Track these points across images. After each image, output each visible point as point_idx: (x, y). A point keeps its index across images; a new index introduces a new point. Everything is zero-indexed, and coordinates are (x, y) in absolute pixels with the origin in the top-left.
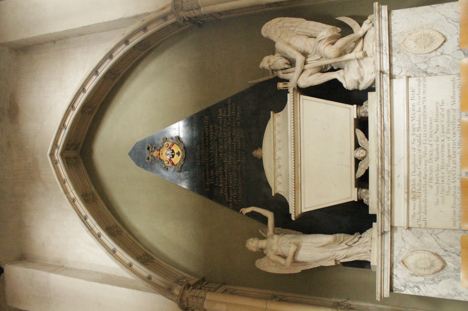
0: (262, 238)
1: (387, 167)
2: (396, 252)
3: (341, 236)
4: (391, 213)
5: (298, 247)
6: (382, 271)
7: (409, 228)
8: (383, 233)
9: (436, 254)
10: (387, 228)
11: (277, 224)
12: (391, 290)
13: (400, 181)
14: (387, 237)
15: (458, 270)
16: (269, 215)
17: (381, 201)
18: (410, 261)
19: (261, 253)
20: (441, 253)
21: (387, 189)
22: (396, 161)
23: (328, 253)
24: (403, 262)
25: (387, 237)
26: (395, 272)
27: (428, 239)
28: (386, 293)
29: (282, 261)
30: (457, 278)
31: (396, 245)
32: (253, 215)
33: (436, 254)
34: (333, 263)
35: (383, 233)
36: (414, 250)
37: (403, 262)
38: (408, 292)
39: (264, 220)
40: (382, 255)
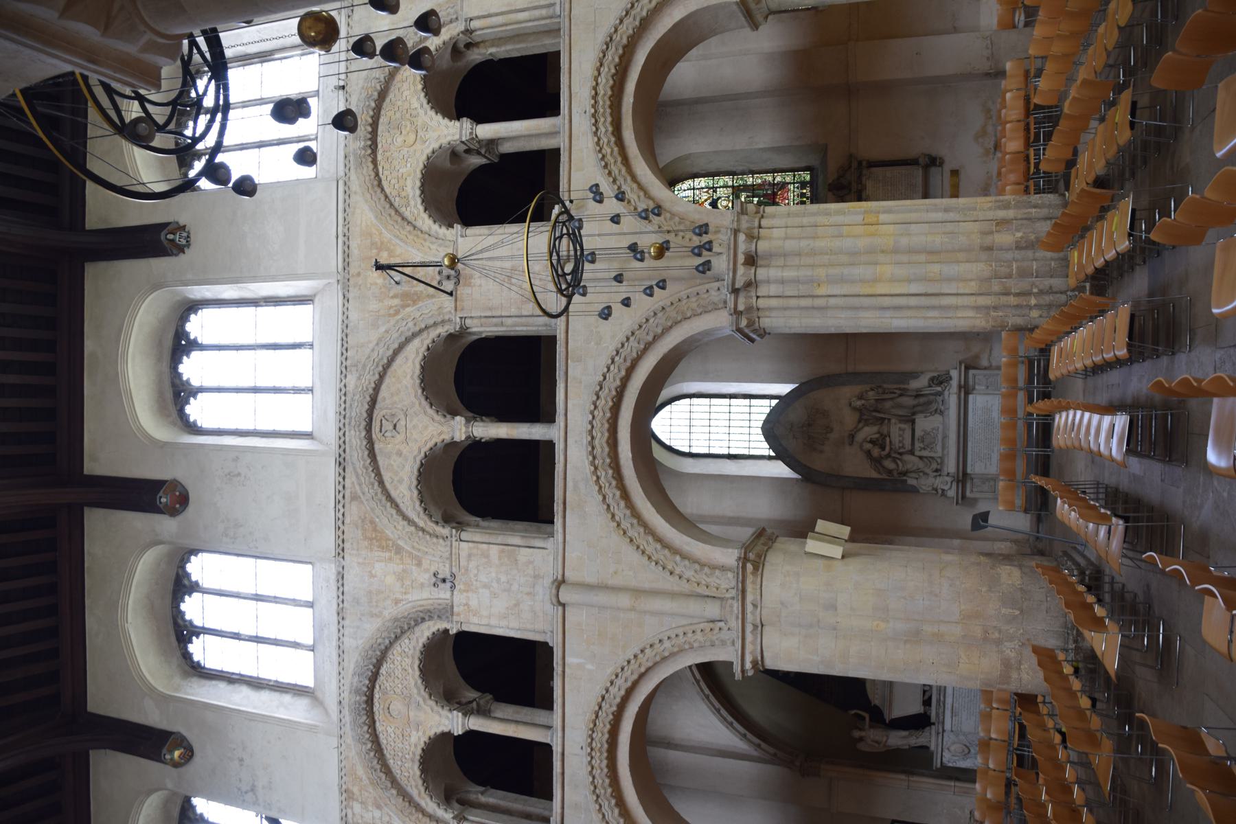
0: (860, 729)
1: (942, 698)
2: (945, 743)
3: (913, 732)
4: (943, 723)
5: (887, 736)
6: (937, 753)
7: (952, 731)
8: (938, 734)
9: (965, 745)
10: (941, 730)
11: (871, 720)
12: (941, 762)
13: (948, 706)
14: (940, 735)
15: (976, 754)
16: (867, 716)
17: (937, 714)
18: (952, 748)
19: (861, 739)
20: (968, 745)
21: (941, 710)
22: (947, 695)
23: (905, 742)
24: (948, 749)
25: (940, 735)
26: (944, 754)
27: (962, 737)
28: (939, 765)
29: (877, 745)
30: (976, 759)
31: (945, 739)
32: (856, 715)
33: (965, 745)
34: (907, 747)
35: (938, 734)
36: (954, 743)
37: (948, 749)
38: (950, 765)
39: (864, 719)
40: (937, 745)
